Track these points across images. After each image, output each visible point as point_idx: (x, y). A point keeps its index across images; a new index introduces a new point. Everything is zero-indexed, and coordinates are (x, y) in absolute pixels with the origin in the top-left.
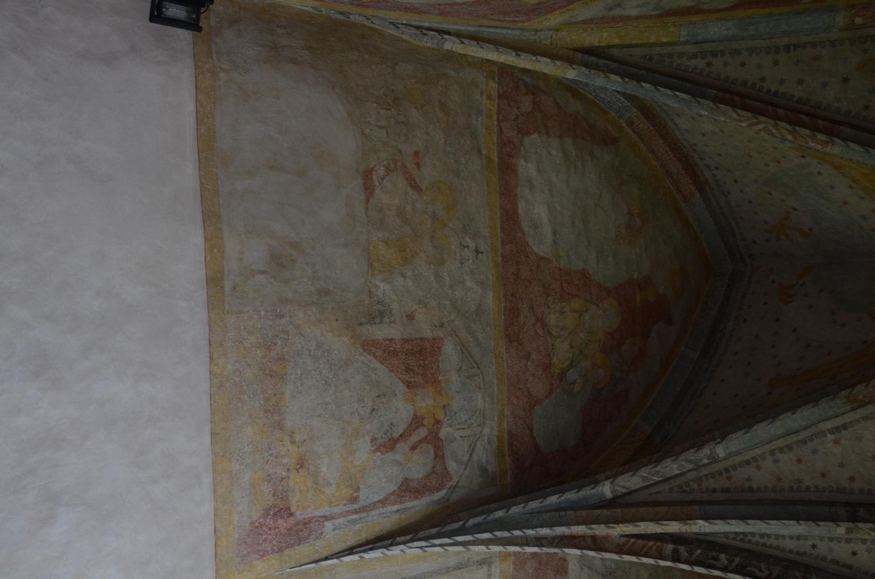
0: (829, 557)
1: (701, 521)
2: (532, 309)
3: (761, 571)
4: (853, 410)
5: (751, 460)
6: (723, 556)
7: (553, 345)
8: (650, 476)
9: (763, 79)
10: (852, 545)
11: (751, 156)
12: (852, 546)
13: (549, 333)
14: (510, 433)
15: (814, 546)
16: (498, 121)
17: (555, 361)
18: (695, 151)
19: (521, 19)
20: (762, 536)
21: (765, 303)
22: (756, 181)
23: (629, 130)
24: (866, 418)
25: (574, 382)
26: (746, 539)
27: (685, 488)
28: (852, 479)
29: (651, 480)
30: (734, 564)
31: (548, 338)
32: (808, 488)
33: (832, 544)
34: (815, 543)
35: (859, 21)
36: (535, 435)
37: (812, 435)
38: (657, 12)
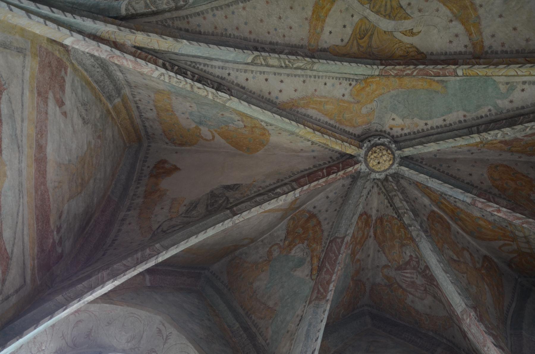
0: (235, 82)
1: (185, 41)
5: (200, 12)
8: (150, 5)
10: (247, 74)
20: (205, 65)
27: (164, 23)
29: (150, 8)
32: (230, 34)
33: (238, 73)
34: (230, 73)
37: (232, 2)
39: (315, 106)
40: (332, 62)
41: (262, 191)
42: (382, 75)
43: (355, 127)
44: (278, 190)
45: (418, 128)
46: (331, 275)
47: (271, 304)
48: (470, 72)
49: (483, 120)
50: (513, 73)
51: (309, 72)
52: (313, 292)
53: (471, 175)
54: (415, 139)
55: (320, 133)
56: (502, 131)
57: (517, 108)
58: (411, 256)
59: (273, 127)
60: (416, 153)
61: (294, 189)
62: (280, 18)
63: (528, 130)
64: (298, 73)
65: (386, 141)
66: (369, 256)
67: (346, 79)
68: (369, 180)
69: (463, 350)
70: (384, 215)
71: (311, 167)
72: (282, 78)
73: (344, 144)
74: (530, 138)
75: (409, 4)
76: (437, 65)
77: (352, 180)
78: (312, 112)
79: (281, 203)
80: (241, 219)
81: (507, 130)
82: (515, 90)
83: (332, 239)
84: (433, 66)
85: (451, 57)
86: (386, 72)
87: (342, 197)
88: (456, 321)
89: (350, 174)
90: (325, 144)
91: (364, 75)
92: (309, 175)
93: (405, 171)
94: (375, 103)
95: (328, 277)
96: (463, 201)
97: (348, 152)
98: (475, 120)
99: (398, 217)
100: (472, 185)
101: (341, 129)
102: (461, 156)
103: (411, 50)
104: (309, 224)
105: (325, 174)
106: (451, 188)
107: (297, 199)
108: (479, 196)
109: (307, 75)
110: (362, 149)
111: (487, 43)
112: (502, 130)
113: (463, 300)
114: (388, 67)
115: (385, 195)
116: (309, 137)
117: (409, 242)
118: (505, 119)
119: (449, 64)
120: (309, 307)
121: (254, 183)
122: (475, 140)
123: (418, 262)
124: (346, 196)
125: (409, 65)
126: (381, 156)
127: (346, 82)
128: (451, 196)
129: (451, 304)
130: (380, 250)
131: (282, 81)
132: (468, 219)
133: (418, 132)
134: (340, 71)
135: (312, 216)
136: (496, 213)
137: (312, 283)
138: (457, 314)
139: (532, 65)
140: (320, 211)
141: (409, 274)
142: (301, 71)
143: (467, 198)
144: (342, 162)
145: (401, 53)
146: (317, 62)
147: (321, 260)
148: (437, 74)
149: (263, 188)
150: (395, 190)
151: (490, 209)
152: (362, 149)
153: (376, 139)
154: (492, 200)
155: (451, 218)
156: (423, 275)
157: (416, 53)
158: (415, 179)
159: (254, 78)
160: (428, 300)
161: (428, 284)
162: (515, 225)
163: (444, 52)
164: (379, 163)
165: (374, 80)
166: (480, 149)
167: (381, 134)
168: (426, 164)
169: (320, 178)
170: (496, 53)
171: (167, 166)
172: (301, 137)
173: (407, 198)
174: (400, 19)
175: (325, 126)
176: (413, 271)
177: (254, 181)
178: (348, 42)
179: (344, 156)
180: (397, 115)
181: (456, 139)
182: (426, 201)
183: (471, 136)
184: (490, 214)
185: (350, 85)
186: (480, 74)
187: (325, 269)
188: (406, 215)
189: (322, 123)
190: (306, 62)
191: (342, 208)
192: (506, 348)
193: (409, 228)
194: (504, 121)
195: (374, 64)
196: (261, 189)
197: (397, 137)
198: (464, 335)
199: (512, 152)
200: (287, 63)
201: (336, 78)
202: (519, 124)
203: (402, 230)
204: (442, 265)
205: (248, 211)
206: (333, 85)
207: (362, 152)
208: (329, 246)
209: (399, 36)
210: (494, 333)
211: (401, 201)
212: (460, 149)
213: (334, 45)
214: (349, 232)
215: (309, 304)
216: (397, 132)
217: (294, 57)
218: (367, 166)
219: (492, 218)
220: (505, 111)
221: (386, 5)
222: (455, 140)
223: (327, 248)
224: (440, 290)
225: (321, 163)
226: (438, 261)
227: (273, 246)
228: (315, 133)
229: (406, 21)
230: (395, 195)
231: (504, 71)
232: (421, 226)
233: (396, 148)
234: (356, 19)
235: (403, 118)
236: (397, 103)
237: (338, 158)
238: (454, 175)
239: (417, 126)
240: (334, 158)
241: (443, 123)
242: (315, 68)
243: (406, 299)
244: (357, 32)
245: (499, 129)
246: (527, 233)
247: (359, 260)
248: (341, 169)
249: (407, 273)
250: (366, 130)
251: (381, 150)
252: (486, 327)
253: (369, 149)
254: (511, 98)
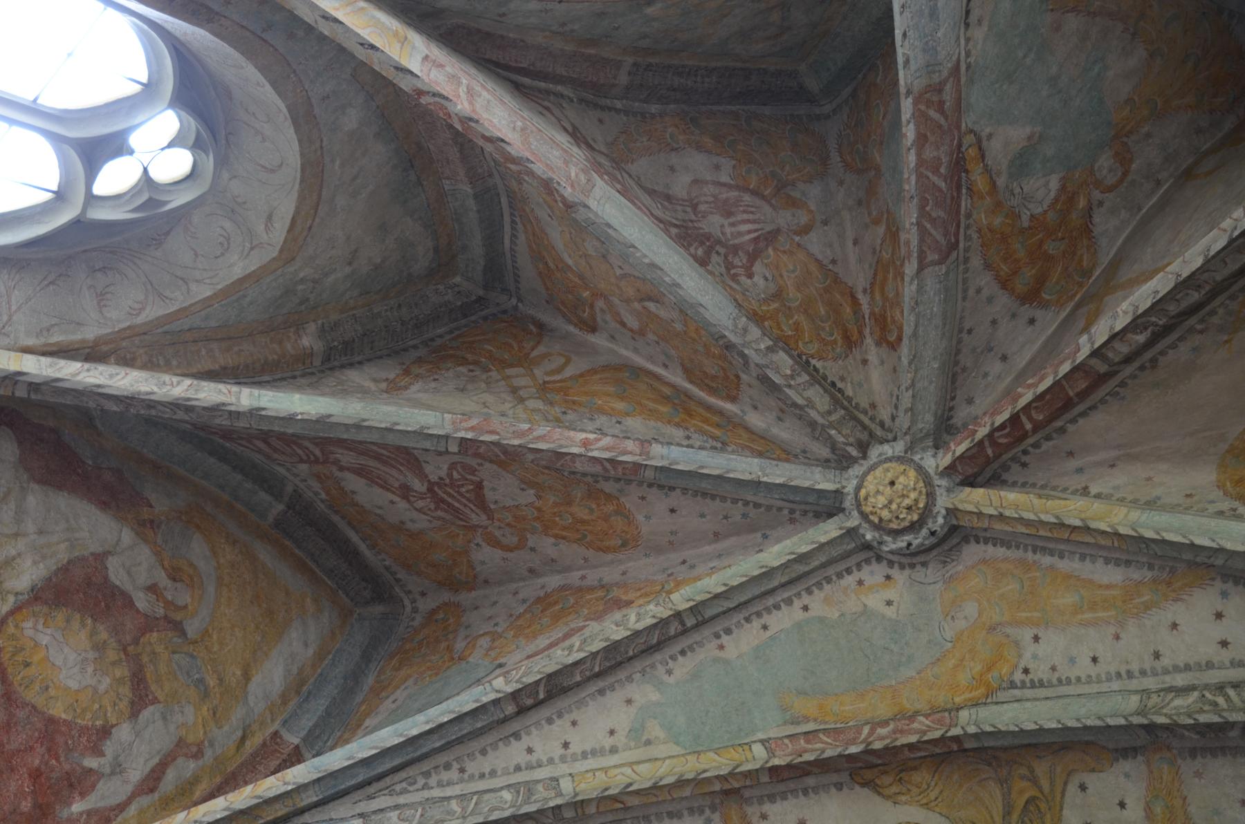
39: (1107, 592)
40: (1089, 723)
41: (1192, 321)
42: (950, 711)
43: (984, 561)
44: (1141, 338)
45: (822, 595)
46: (921, 162)
47: (1073, 23)
48: (736, 756)
49: (679, 648)
50: (641, 768)
51: (1150, 683)
52: (959, 100)
53: (672, 511)
54: (823, 566)
55: (1067, 523)
56: (628, 629)
57: (612, 688)
58: (750, 276)
59: (1212, 509)
60: (811, 531)
61: (1095, 353)
63: (577, 644)
64: (1183, 675)
65: (891, 545)
66: (855, 242)
67: (1041, 684)
68: (906, 434)
69: (572, 101)
70: (847, 356)
71: (1071, 428)
72: (1225, 656)
73: (996, 508)
74: (573, 625)
76: (815, 760)
77: (951, 422)
78: (1112, 575)
79: (1124, 305)
80: (1227, 223)
81: (619, 634)
82: (627, 730)
83: (954, 254)
84: (825, 755)
85: (792, 785)
86: (940, 722)
87: (964, 370)
88: (603, 160)
89: (959, 437)
90: (1048, 497)
91: (997, 703)
92: (1068, 404)
93: (824, 481)
94: (949, 635)
95: (929, 153)
96: (669, 444)
97: (981, 491)
98: (696, 643)
99: (808, 362)
100: (661, 487)
101: (1018, 547)
102: (708, 548)
103: (894, 789)
104: (1034, 271)
105: (1024, 419)
106: (702, 467)
107: (1086, 329)
108: (637, 467)
109: (1155, 674)
110: (947, 509)
112: (629, 633)
113: (596, 214)
114: (937, 734)
115: (857, 407)
116: (1098, 506)
117: (764, 308)
118: (631, 658)
119: (789, 766)
120: (955, 58)
121: (1226, 338)
122: (681, 595)
123: (729, 266)
124: (954, 375)
125: (886, 748)
126: (890, 502)
127: (1041, 675)
128: (701, 448)
129: (623, 195)
130: (830, 267)
131: (1224, 644)
132: (651, 405)
133: (819, 585)
134: (1062, 701)
135: (1031, 296)
136: (592, 436)
137: (968, 121)
138: (602, 179)
139: (606, 793)
140: (1014, 316)
141: (743, 230)
142: (1174, 684)
143: (662, 455)
144: (988, 462)
145: (917, 777)
146: (1131, 715)
147: (964, 191)
148: (811, 737)
149: (1191, 330)
150: (831, 426)
151: (607, 441)
152: (947, 509)
153: (916, 542)
154: (608, 465)
155: (689, 396)
156: (708, 239)
157: (878, 782)
158: (793, 466)
160: (680, 186)
161: (692, 221)
162: (548, 420)
163: (812, 795)
164: (892, 483)
165: (967, 695)
166: (669, 575)
167: (912, 558)
168: (780, 509)
169: (1034, 405)
170: (691, 811)
172: (1122, 500)
173: (789, 410)
175: (1062, 547)
176: (736, 241)
177: (1226, 342)
178: (1066, 784)
179: (989, 480)
180: (883, 616)
181: (724, 589)
182: (756, 420)
183: (692, 603)
184: (605, 430)
185: (1026, 671)
186: (711, 755)
187: (943, 170)
188: (789, 372)
189: (1074, 553)
190: (1165, 711)
191: (954, 342)
192: (481, 142)
193: (771, 343)
194: (631, 653)
195: (976, 736)
196: (1199, 327)
197: (868, 561)
198: (576, 135)
199: (603, 587)
200: (1221, 700)
201: (1069, 682)
202: (598, 652)
203: (790, 333)
204: (667, 279)
205: (1212, 253)
206: (1072, 660)
207: (943, 502)
208: (957, 234)
210: (513, 167)
211: (810, 401)
212: (712, 565)
213: (1101, 772)
214: (914, 287)
215: (957, 68)
216: (872, 573)
217: (1203, 718)
218: (920, 469)
219: (598, 424)
220: (637, 676)
222: (725, 585)
223: (958, 226)
224: (657, 218)
225: (1046, 446)
226: (678, 286)
227: (1121, 181)
228: (1082, 520)
230: (829, 413)
231: (662, 770)
232: (743, 356)
233: (861, 531)
235: (866, 611)
236: (892, 646)
237: (1005, 468)
238: (708, 501)
239: (827, 601)
240: (1015, 467)
241: (766, 619)
242: (1135, 699)
243: (734, 167)
244: (1048, 816)
245: (637, 634)
246: (520, 410)
247: (876, 222)
248: (987, 443)
249: (749, 232)
250: (953, 560)
251: (897, 518)
252: (531, 173)
253: (926, 513)
254: (632, 710)
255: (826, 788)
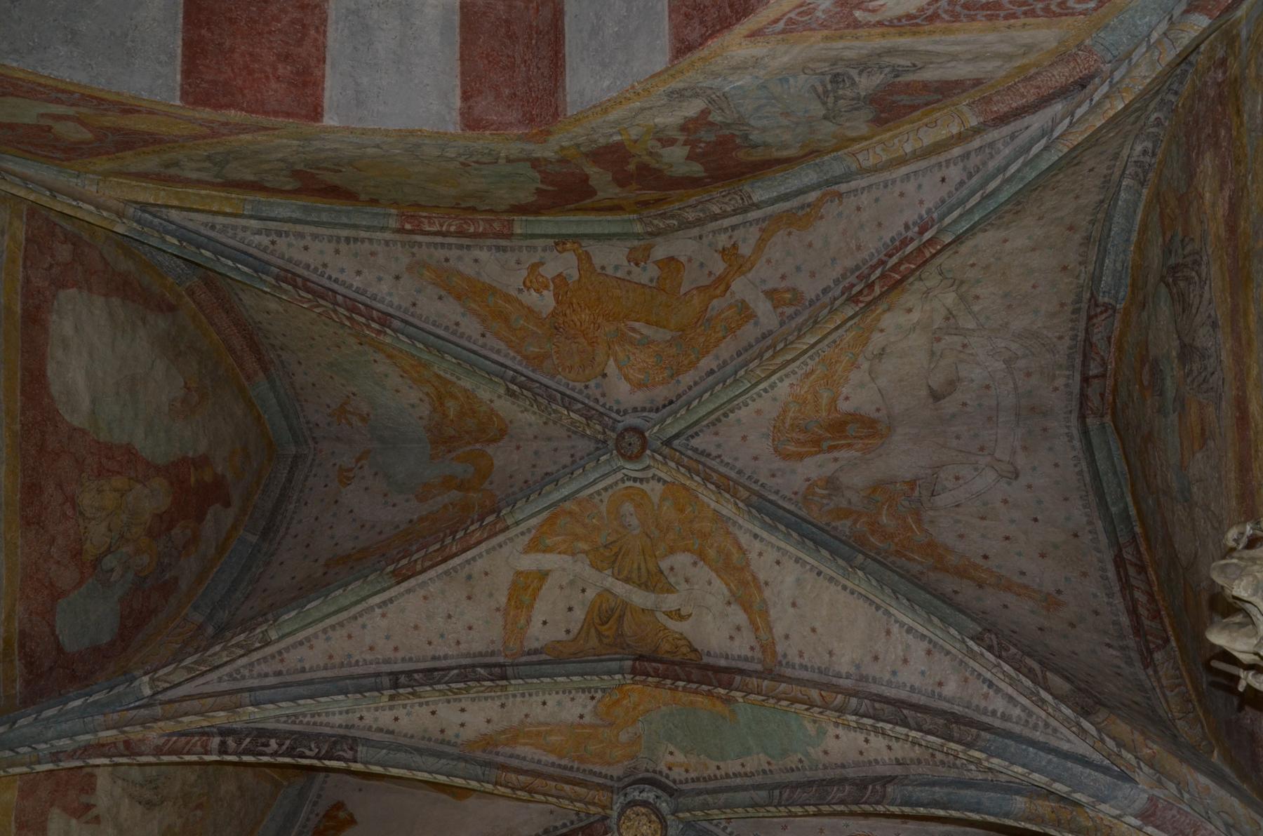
2: (60, 486)
3: (311, 750)
4: (398, 583)
6: (273, 742)
7: (86, 528)
9: (325, 265)
11: (313, 339)
12: (395, 712)
13: (81, 513)
14: (23, 633)
15: (361, 718)
16: (25, 267)
17: (88, 546)
18: (259, 329)
19: (58, 156)
20: (313, 716)
21: (326, 486)
22: (319, 365)
23: (187, 299)
24: (409, 591)
25: (112, 570)
26: (297, 721)
28: (396, 649)
30: (284, 747)
31: (81, 521)
32: (357, 662)
33: (377, 713)
35: (408, 227)
36: (57, 632)
38: (219, 180)
43: (609, 764)
45: (709, 772)
62: (450, 617)
72: (463, 704)
75: (672, 569)
111: (779, 649)
127: (583, 696)
153: (636, 793)
159: (408, 714)
171: (342, 815)
174: (662, 591)
178: (579, 633)
185: (593, 698)
206: (559, 703)
209: (663, 619)
221: (639, 569)
229: (670, 596)
234: (591, 594)
255: (716, 656)
